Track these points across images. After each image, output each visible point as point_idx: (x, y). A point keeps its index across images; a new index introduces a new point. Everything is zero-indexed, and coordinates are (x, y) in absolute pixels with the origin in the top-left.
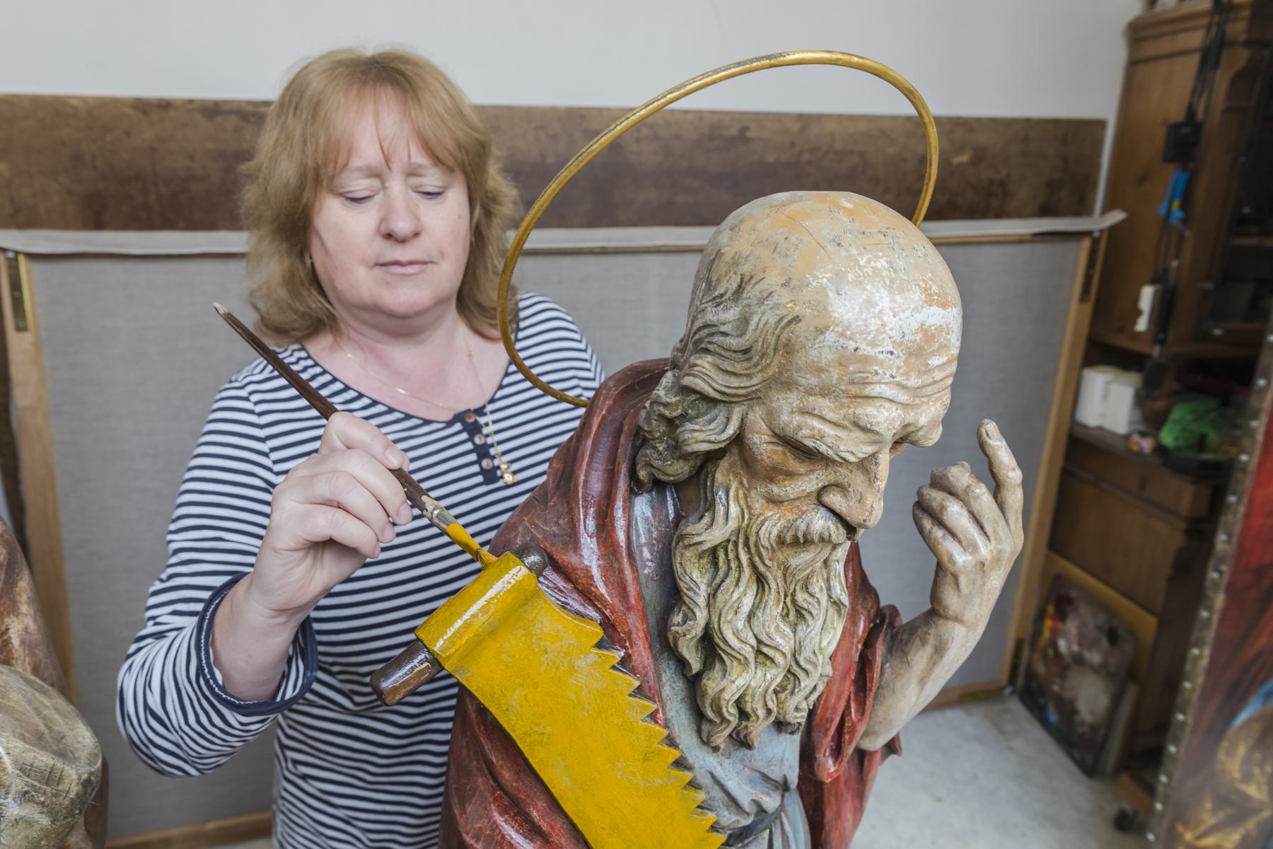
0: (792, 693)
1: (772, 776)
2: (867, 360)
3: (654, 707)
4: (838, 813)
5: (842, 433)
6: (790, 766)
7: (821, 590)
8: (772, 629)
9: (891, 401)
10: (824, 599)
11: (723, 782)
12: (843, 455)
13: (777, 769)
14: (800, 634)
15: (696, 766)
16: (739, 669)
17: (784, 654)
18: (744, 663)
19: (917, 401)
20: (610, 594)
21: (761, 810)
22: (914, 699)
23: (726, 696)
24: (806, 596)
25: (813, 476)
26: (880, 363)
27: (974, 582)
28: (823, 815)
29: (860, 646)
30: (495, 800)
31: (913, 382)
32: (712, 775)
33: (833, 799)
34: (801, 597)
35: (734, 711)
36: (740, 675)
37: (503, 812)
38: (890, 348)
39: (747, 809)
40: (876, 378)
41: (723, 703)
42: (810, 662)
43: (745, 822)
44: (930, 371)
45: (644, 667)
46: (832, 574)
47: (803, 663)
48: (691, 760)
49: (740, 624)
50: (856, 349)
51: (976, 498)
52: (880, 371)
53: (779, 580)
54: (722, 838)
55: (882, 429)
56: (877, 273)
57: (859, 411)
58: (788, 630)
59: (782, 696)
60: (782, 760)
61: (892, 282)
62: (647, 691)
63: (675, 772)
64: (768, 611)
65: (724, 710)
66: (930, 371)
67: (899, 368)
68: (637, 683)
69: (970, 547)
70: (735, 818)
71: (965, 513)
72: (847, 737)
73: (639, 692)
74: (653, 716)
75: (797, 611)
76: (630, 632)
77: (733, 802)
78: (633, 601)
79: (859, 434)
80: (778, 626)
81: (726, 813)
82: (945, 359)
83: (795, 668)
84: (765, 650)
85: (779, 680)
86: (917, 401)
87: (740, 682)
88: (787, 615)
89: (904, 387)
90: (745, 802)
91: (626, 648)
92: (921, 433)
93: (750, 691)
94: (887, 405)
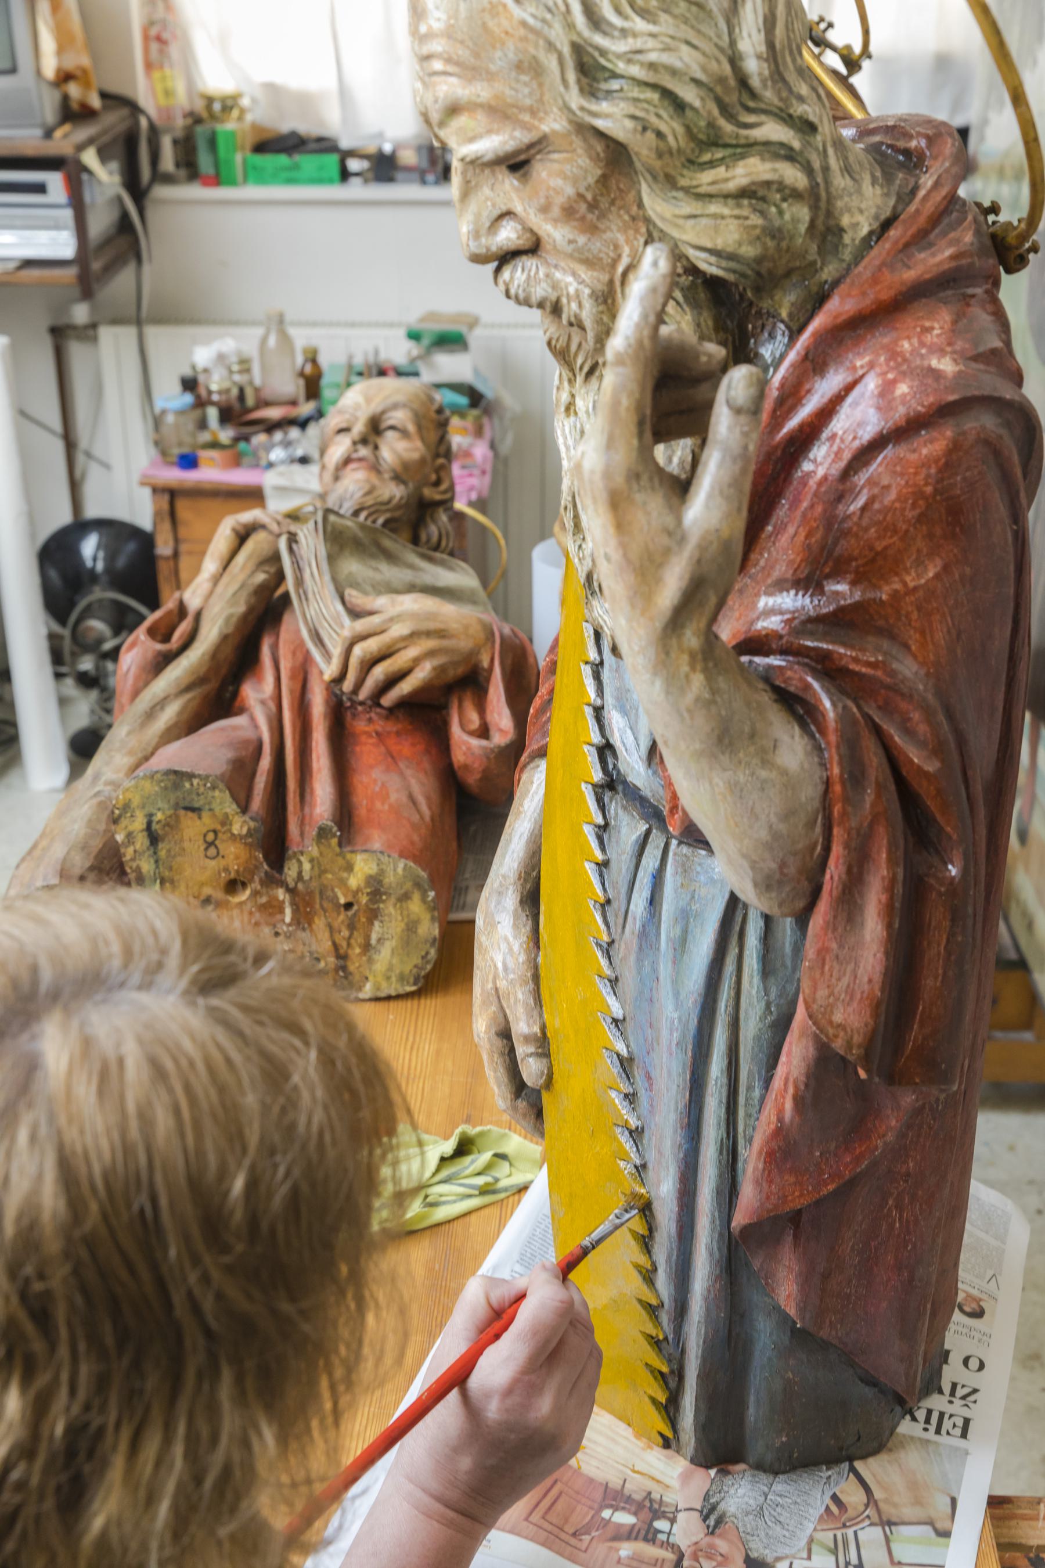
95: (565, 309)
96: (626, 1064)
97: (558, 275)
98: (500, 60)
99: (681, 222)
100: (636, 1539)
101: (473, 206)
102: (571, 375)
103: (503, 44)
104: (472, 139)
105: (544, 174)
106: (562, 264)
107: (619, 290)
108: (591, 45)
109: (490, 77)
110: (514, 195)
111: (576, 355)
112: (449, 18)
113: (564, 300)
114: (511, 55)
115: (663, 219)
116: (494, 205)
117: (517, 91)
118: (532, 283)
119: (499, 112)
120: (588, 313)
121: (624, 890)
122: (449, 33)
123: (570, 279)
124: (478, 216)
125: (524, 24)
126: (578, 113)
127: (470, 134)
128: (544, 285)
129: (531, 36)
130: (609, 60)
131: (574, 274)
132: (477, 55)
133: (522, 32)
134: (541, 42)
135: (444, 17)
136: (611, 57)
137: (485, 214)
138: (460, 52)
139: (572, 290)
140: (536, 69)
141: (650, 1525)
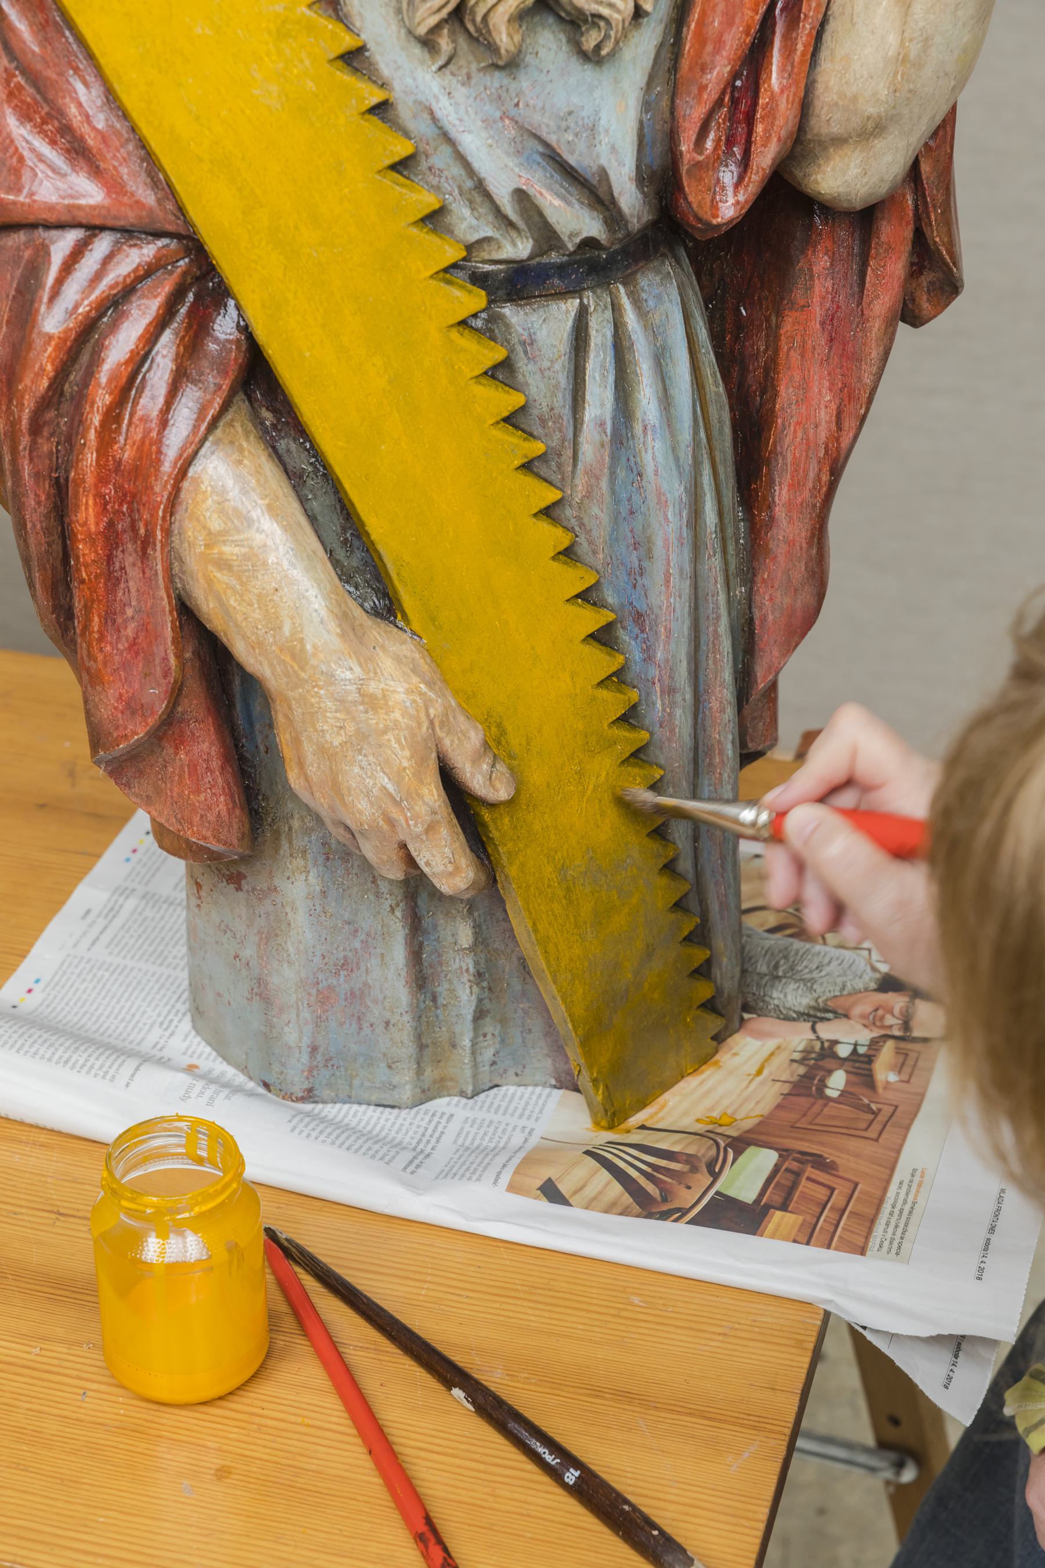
1: (572, 160)
4: (805, 386)
6: (613, 149)
11: (454, 134)
13: (581, 146)
15: (397, 85)
21: (548, 237)
22: (893, 40)
28: (776, 395)
30: (11, 95)
32: (431, 113)
33: (795, 355)
37: (25, 115)
39: (509, 209)
43: (519, 248)
48: (385, 70)
54: (453, 254)
60: (593, 129)
63: (344, 77)
70: (488, 231)
72: (759, 128)
77: (481, 188)
81: (466, 212)
90: (502, 192)
96: (603, 638)
100: (870, 1070)
121: (567, 412)
141: (845, 1059)
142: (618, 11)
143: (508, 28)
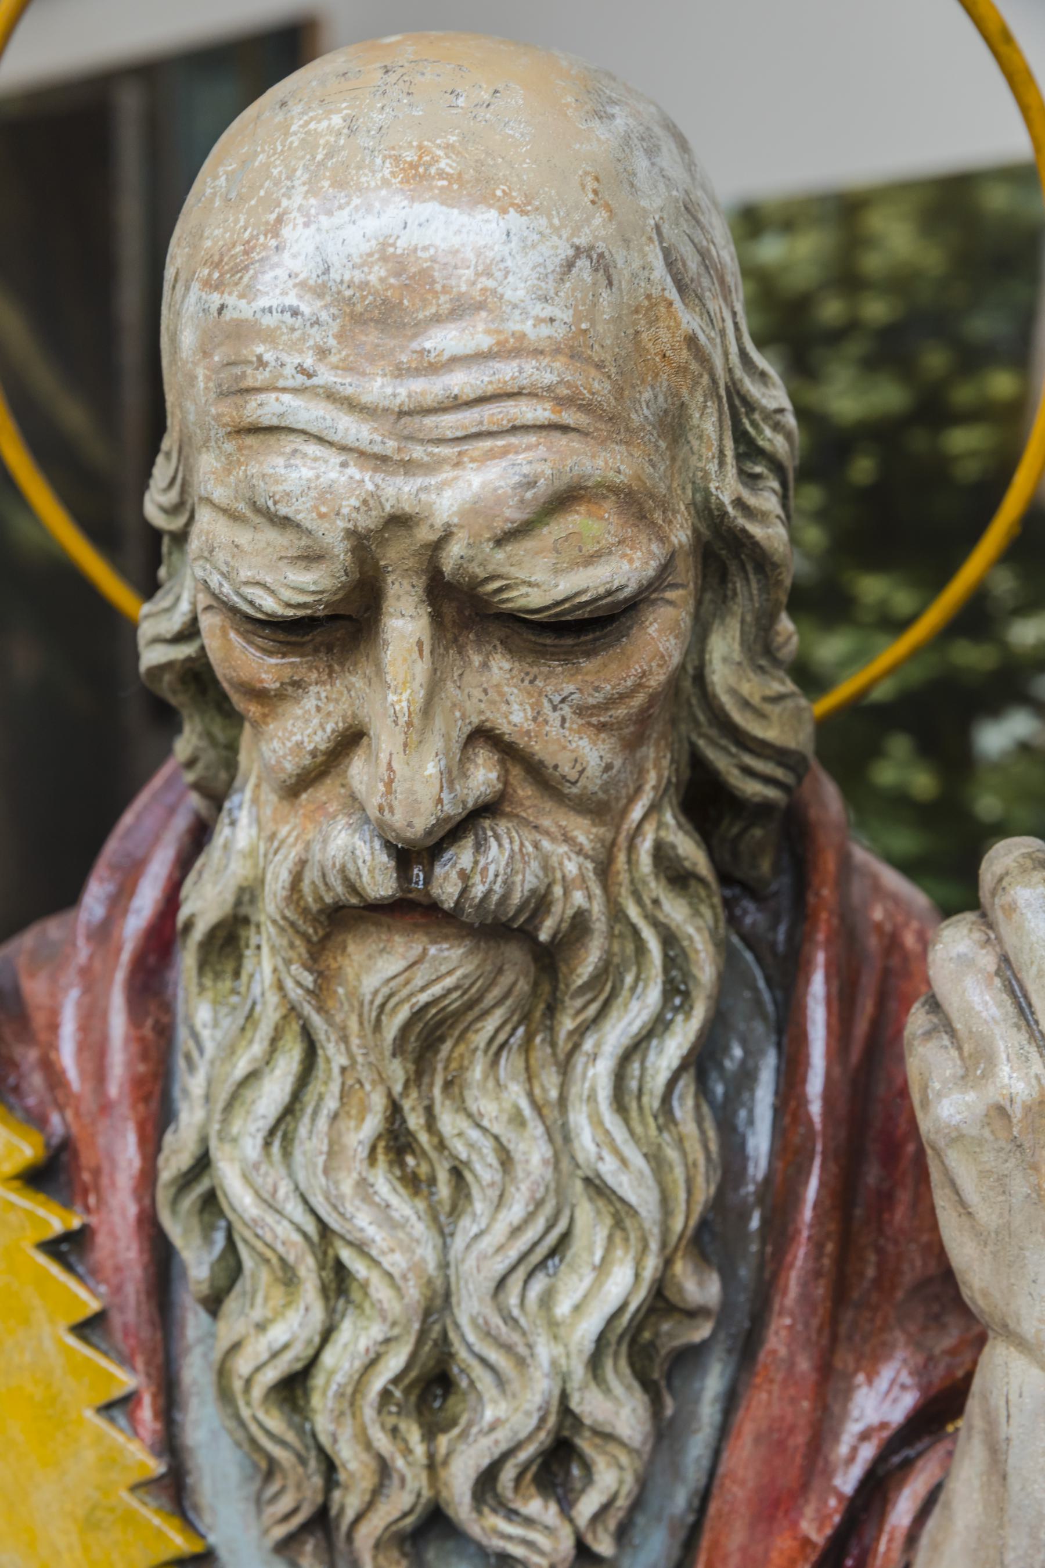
0: (464, 1435)
2: (242, 331)
3: (126, 1380)
5: (244, 537)
7: (518, 1120)
8: (347, 1187)
9: (320, 440)
10: (533, 1152)
12: (250, 591)
14: (458, 1243)
16: (278, 1294)
17: (390, 1275)
18: (288, 1277)
19: (418, 452)
20: (82, 1073)
23: (243, 1365)
24: (464, 1124)
25: (309, 703)
26: (269, 337)
27: (1002, 1183)
29: (867, 1452)
31: (379, 388)
34: (449, 1122)
35: (275, 1422)
36: (279, 1314)
38: (291, 300)
40: (261, 377)
41: (238, 1385)
42: (488, 1334)
44: (434, 367)
45: (118, 1269)
46: (574, 1091)
47: (471, 1337)
49: (251, 1147)
50: (222, 308)
51: (1011, 909)
52: (268, 357)
53: (355, 1041)
55: (301, 510)
56: (309, 143)
57: (253, 469)
58: (404, 1206)
59: (443, 1441)
61: (329, 156)
62: (119, 1335)
64: (322, 1123)
65: (245, 1413)
66: (434, 367)
67: (323, 353)
68: (94, 1305)
69: (977, 1063)
71: (988, 961)
73: (90, 1328)
74: (123, 1405)
75: (457, 1174)
76: (97, 1172)
78: (114, 1090)
79: (271, 535)
80: (363, 1185)
82: (485, 342)
83: (463, 1354)
84: (346, 1255)
85: (395, 1362)
86: (418, 452)
87: (278, 1334)
88: (432, 1181)
89: (352, 405)
91: (87, 1210)
92: (455, 551)
93: (318, 1380)
94: (312, 449)
95: (557, 909)
97: (546, 844)
98: (645, 405)
99: (768, 708)
101: (439, 723)
102: (411, 1067)
103: (656, 375)
104: (591, 560)
105: (653, 630)
106: (546, 823)
107: (621, 858)
108: (738, 393)
109: (628, 435)
110: (513, 692)
111: (486, 1013)
112: (578, 317)
113: (558, 891)
114: (661, 398)
115: (746, 704)
116: (463, 717)
117: (653, 466)
118: (519, 866)
119: (636, 505)
120: (597, 909)
122: (574, 350)
123: (564, 848)
124: (447, 737)
125: (691, 340)
126: (730, 509)
127: (591, 548)
128: (534, 865)
129: (694, 366)
130: (753, 423)
131: (567, 839)
132: (619, 392)
133: (685, 353)
134: (705, 380)
135: (567, 316)
136: (757, 416)
137: (455, 734)
138: (596, 386)
139: (571, 867)
140: (674, 426)
142: (542, 1553)
143: (375, 1558)
